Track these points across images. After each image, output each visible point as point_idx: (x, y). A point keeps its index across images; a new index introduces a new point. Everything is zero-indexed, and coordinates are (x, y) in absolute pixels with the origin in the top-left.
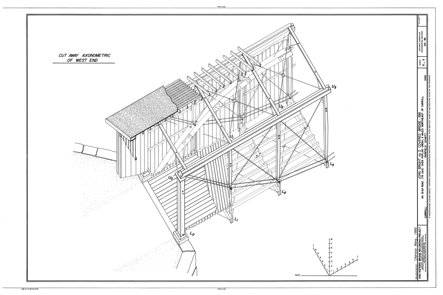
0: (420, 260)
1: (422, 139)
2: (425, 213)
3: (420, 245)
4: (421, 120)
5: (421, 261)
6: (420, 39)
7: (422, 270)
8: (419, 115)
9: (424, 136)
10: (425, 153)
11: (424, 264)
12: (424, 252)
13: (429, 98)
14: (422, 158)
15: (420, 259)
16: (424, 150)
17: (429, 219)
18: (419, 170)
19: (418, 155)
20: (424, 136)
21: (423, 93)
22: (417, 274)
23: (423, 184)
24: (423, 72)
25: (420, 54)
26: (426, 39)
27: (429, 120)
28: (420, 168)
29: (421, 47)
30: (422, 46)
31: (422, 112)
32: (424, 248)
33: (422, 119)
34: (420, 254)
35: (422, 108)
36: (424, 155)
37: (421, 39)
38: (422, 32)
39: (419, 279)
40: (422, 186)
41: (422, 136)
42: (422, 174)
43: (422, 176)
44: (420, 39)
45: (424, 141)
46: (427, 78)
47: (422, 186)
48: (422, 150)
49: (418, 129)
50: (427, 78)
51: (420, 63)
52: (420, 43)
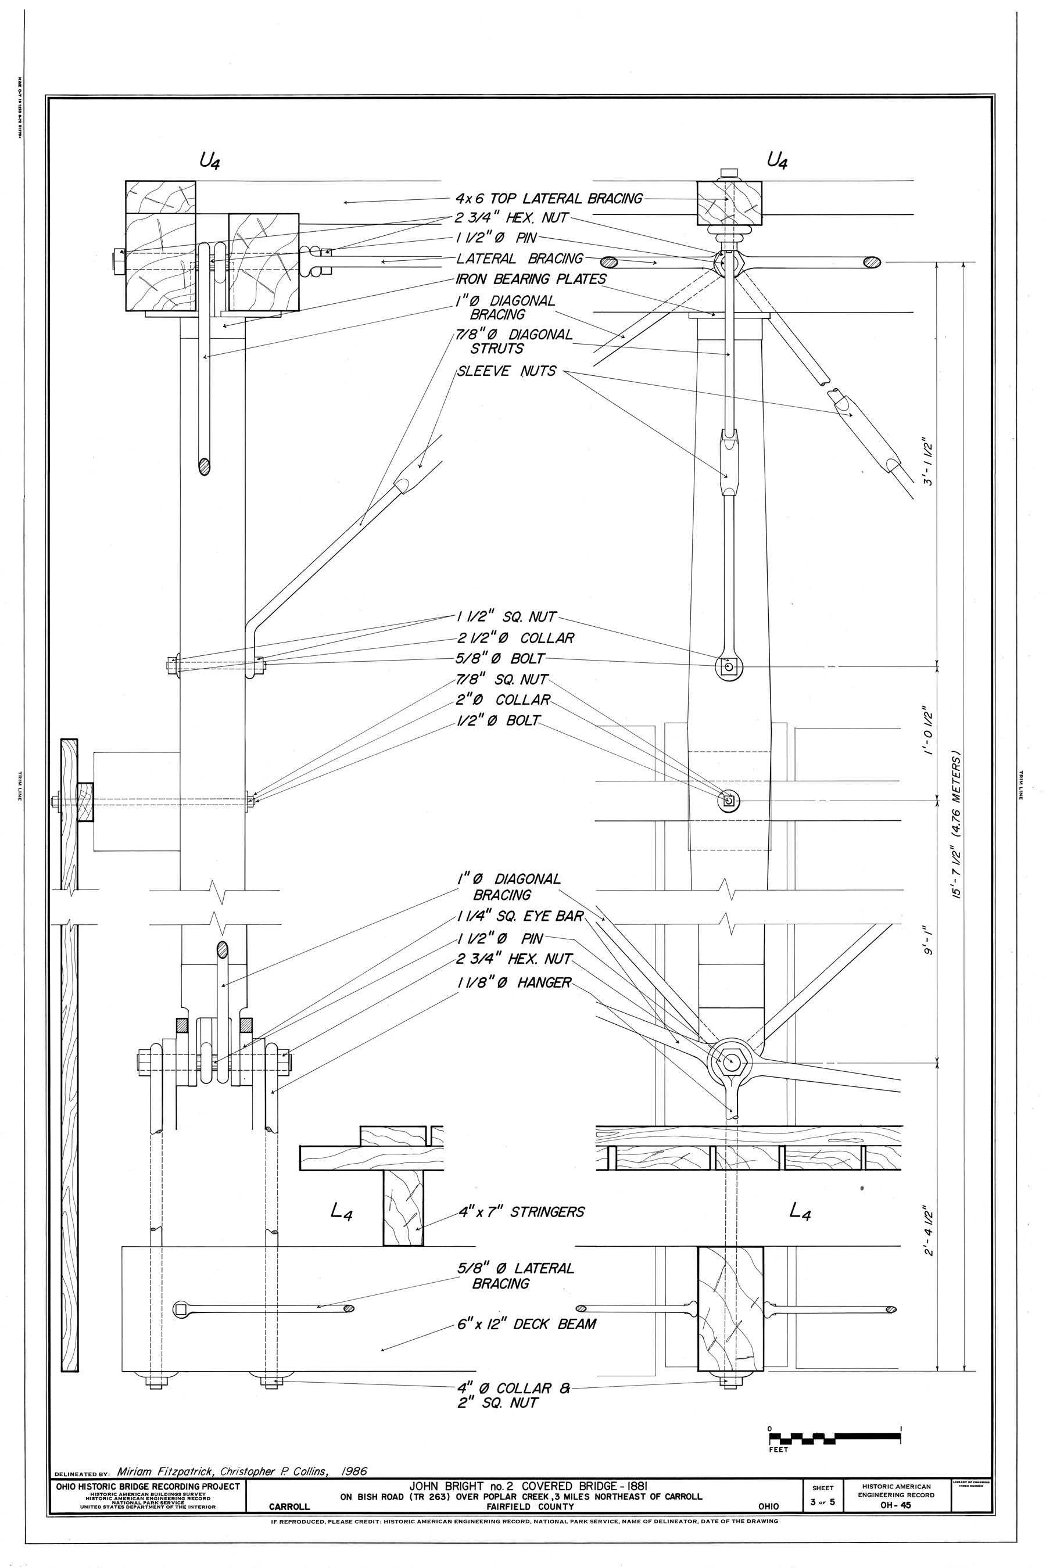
0: (122, 1487)
1: (552, 1494)
2: (290, 1506)
3: (176, 1486)
4: (620, 1491)
5: (118, 1491)
6: (906, 1487)
7: (87, 1493)
8: (638, 1483)
9: (562, 1501)
10: (502, 1506)
11: (109, 1503)
12: (152, 1501)
13: (699, 1519)
14: (486, 1496)
15: (128, 1486)
16: (513, 1501)
17: (269, 1519)
18: (442, 1484)
19: (496, 1482)
20: (562, 1501)
21: (715, 1497)
22: (74, 1477)
23: (395, 1497)
24: (319, 1496)
25: (854, 1488)
26: (906, 1510)
27: (620, 1519)
28: (584, 1486)
29: (877, 1491)
30: (880, 1495)
31: (648, 1493)
32: (166, 1500)
33: (624, 1496)
34: (145, 1487)
35: (662, 1496)
36: (497, 1501)
37: (905, 1491)
38: (932, 1495)
39: (54, 1483)
40: (384, 1496)
41: (562, 1494)
42: (427, 1497)
43: (422, 1496)
44: (906, 1487)
45: (544, 1502)
46: (769, 1512)
47: (384, 1496)
48: (514, 1496)
49: (586, 1482)
50: (769, 1512)
51: (822, 1488)
52: (890, 1487)
